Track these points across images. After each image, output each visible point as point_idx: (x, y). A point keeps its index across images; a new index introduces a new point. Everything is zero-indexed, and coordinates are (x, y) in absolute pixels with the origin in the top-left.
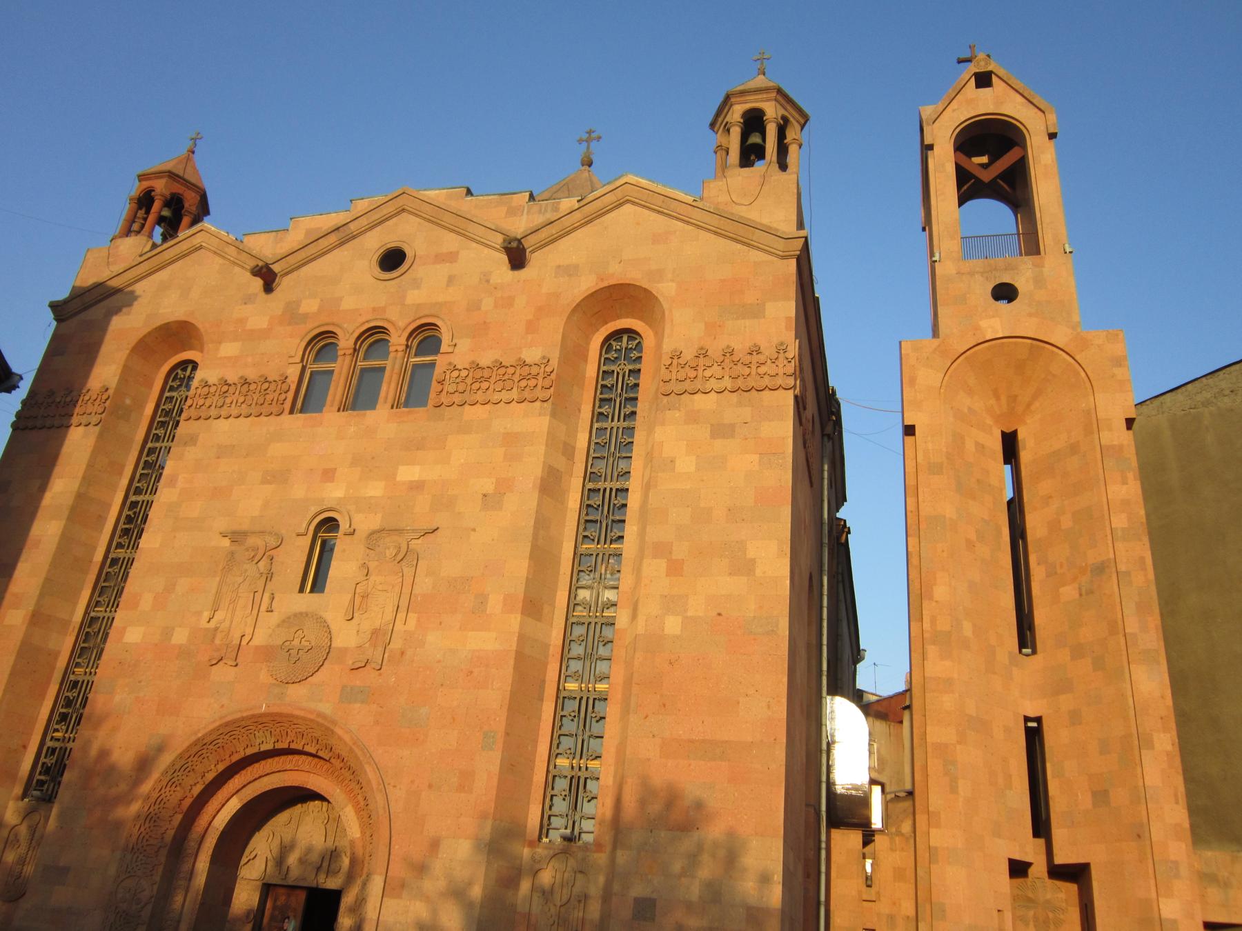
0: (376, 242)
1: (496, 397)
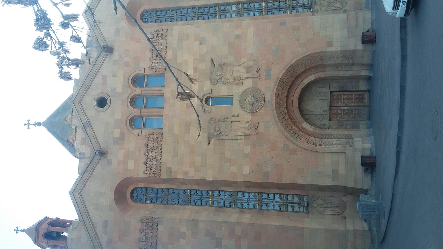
1: (164, 47)
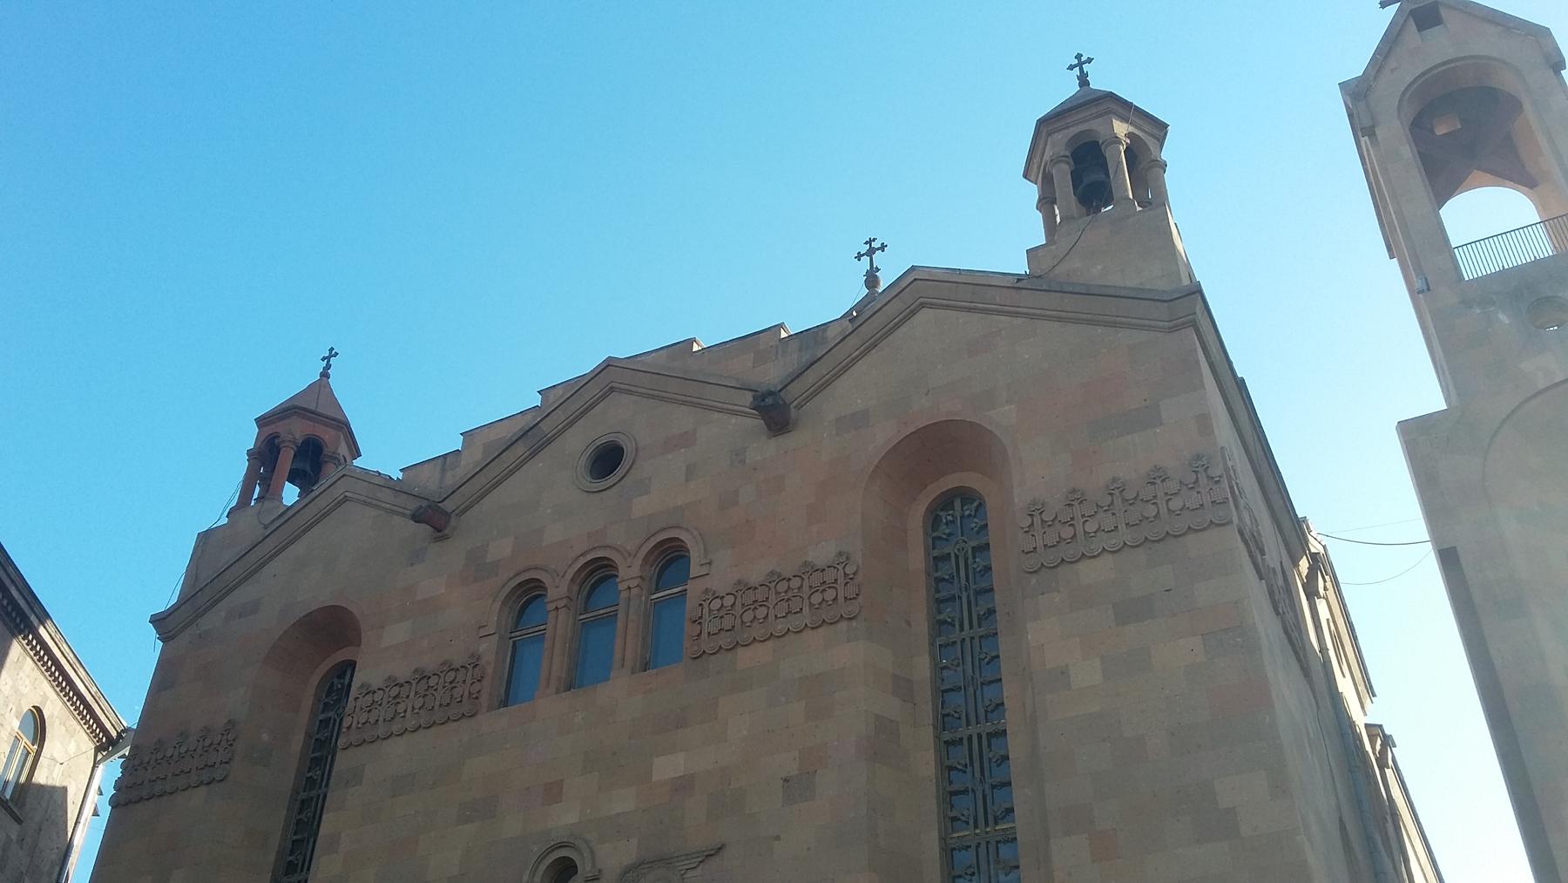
0: (579, 443)
1: (780, 626)
